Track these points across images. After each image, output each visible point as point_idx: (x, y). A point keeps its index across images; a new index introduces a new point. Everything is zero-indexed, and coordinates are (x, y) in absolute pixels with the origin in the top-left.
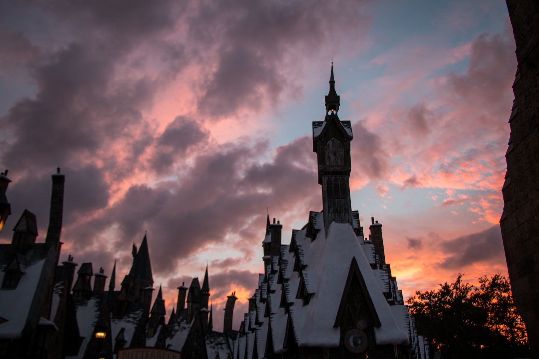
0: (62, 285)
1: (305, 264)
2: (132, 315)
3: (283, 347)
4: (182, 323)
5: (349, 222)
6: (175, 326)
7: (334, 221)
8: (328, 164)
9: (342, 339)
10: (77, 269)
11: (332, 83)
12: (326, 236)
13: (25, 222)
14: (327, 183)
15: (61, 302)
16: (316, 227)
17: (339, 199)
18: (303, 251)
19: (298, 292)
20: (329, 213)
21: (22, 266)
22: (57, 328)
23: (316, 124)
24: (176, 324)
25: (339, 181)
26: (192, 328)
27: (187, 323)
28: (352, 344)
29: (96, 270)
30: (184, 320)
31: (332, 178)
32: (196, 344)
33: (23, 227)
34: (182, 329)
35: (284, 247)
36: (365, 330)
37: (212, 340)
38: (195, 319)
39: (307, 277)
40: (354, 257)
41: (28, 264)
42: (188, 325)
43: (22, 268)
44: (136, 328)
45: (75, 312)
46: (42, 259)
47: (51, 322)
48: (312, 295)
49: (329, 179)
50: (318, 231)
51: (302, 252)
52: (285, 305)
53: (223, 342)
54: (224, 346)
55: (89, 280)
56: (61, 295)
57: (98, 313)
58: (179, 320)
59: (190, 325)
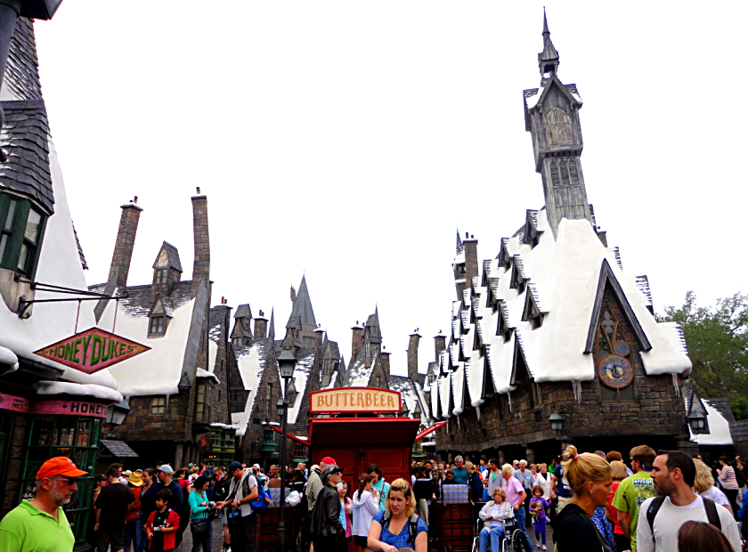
0: (219, 330)
1: (527, 277)
2: (302, 362)
3: (511, 385)
8: (550, 142)
10: (233, 313)
11: (546, 33)
12: (555, 237)
13: (165, 257)
15: (219, 350)
16: (539, 229)
19: (524, 313)
21: (168, 309)
22: (218, 380)
23: (528, 93)
27: (366, 368)
28: (610, 376)
29: (255, 315)
33: (163, 263)
36: (628, 357)
37: (397, 386)
40: (605, 259)
41: (173, 306)
43: (169, 311)
44: (307, 376)
45: (236, 362)
46: (191, 299)
47: (210, 373)
48: (543, 315)
50: (540, 233)
52: (505, 331)
53: (409, 387)
54: (410, 392)
55: (248, 325)
56: (218, 343)
57: (264, 361)
58: (356, 365)
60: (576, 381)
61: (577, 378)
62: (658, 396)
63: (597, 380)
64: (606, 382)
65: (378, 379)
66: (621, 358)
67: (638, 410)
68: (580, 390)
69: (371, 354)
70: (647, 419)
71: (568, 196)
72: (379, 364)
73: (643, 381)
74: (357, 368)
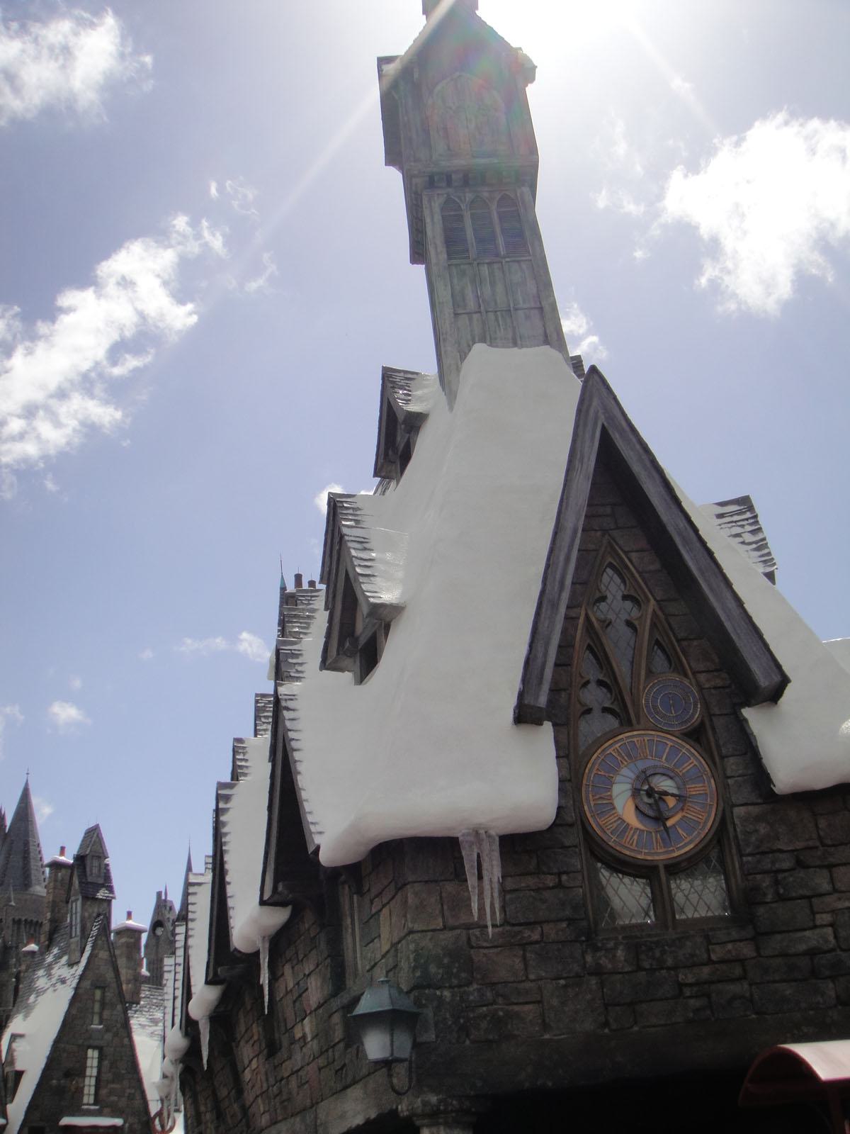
3: (263, 903)
4: (56, 967)
5: (546, 341)
6: (38, 978)
7: (483, 340)
9: (570, 783)
14: (442, 216)
17: (496, 266)
18: (358, 513)
20: (456, 315)
24: (41, 972)
25: (494, 207)
26: (82, 977)
27: (71, 964)
30: (61, 957)
31: (461, 200)
32: (101, 1027)
34: (54, 985)
35: (312, 597)
36: (695, 735)
38: (93, 948)
39: (365, 549)
42: (73, 971)
49: (449, 204)
51: (357, 515)
58: (49, 959)
59: (76, 971)
60: (477, 834)
61: (481, 819)
62: (826, 887)
63: (572, 838)
64: (612, 840)
65: (98, 994)
66: (671, 741)
67: (747, 950)
68: (494, 870)
69: (83, 929)
70: (788, 990)
71: (493, 284)
72: (103, 955)
73: (763, 829)
74: (50, 967)
